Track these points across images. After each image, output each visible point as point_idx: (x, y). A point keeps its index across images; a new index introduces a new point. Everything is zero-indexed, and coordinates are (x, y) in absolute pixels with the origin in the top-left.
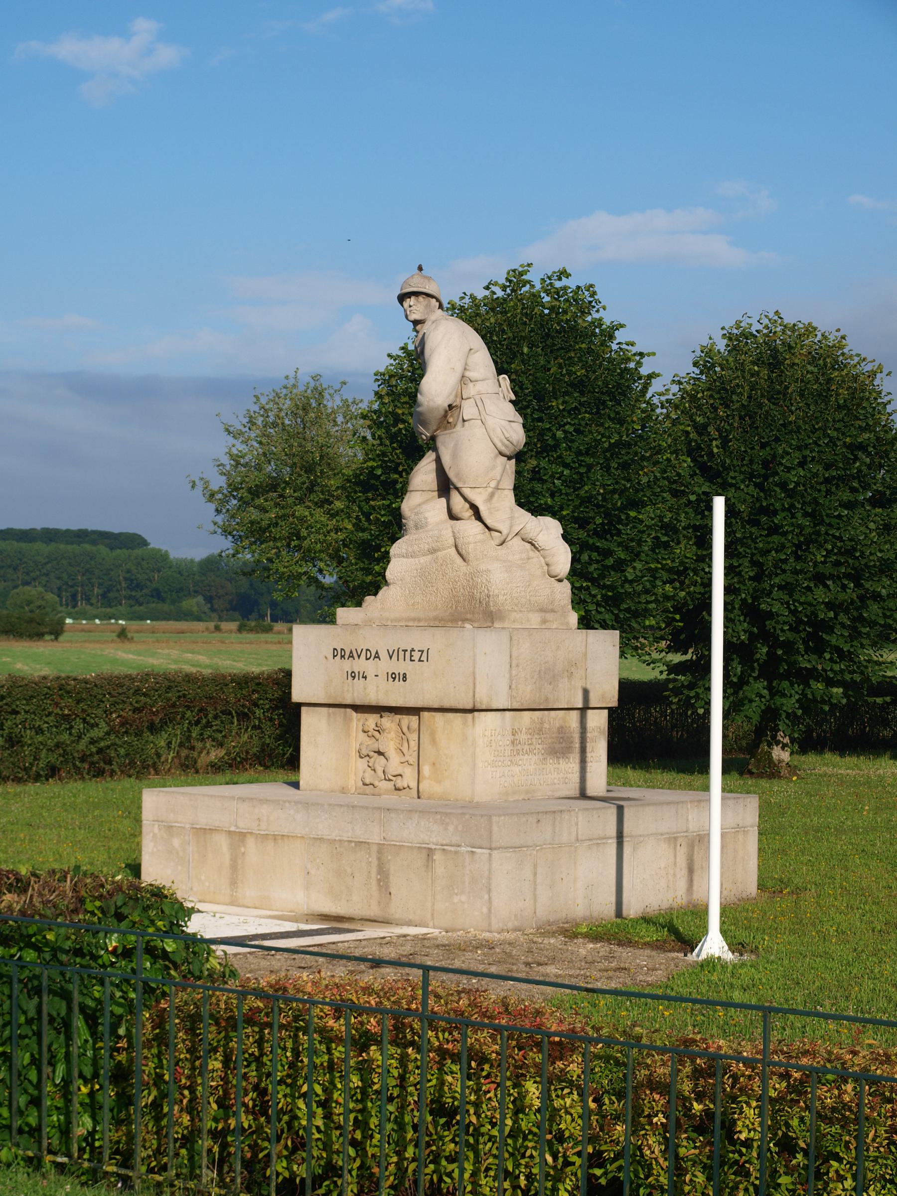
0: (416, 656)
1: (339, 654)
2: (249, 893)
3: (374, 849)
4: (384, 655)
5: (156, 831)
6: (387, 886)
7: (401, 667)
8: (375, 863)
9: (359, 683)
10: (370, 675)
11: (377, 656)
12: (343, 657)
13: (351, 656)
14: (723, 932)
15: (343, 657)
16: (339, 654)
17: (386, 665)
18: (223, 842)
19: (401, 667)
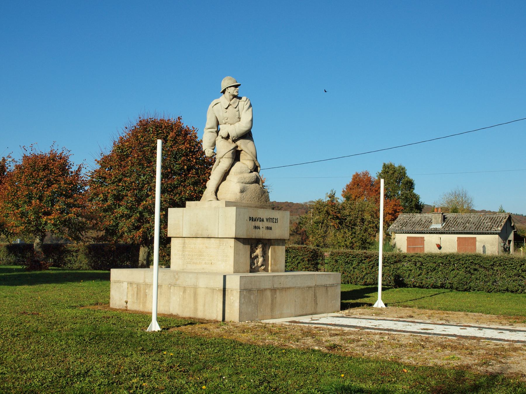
0: (274, 220)
1: (251, 219)
2: (277, 313)
3: (313, 288)
4: (265, 220)
5: (245, 293)
6: (316, 301)
7: (270, 224)
8: (313, 294)
9: (257, 230)
10: (261, 227)
11: (263, 221)
12: (252, 220)
13: (255, 220)
14: (382, 300)
15: (252, 220)
16: (251, 219)
17: (266, 224)
18: (268, 294)
19: (270, 224)
